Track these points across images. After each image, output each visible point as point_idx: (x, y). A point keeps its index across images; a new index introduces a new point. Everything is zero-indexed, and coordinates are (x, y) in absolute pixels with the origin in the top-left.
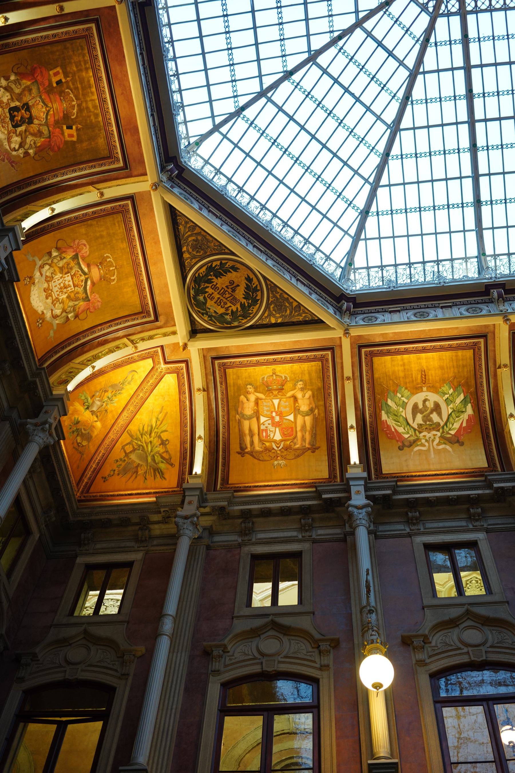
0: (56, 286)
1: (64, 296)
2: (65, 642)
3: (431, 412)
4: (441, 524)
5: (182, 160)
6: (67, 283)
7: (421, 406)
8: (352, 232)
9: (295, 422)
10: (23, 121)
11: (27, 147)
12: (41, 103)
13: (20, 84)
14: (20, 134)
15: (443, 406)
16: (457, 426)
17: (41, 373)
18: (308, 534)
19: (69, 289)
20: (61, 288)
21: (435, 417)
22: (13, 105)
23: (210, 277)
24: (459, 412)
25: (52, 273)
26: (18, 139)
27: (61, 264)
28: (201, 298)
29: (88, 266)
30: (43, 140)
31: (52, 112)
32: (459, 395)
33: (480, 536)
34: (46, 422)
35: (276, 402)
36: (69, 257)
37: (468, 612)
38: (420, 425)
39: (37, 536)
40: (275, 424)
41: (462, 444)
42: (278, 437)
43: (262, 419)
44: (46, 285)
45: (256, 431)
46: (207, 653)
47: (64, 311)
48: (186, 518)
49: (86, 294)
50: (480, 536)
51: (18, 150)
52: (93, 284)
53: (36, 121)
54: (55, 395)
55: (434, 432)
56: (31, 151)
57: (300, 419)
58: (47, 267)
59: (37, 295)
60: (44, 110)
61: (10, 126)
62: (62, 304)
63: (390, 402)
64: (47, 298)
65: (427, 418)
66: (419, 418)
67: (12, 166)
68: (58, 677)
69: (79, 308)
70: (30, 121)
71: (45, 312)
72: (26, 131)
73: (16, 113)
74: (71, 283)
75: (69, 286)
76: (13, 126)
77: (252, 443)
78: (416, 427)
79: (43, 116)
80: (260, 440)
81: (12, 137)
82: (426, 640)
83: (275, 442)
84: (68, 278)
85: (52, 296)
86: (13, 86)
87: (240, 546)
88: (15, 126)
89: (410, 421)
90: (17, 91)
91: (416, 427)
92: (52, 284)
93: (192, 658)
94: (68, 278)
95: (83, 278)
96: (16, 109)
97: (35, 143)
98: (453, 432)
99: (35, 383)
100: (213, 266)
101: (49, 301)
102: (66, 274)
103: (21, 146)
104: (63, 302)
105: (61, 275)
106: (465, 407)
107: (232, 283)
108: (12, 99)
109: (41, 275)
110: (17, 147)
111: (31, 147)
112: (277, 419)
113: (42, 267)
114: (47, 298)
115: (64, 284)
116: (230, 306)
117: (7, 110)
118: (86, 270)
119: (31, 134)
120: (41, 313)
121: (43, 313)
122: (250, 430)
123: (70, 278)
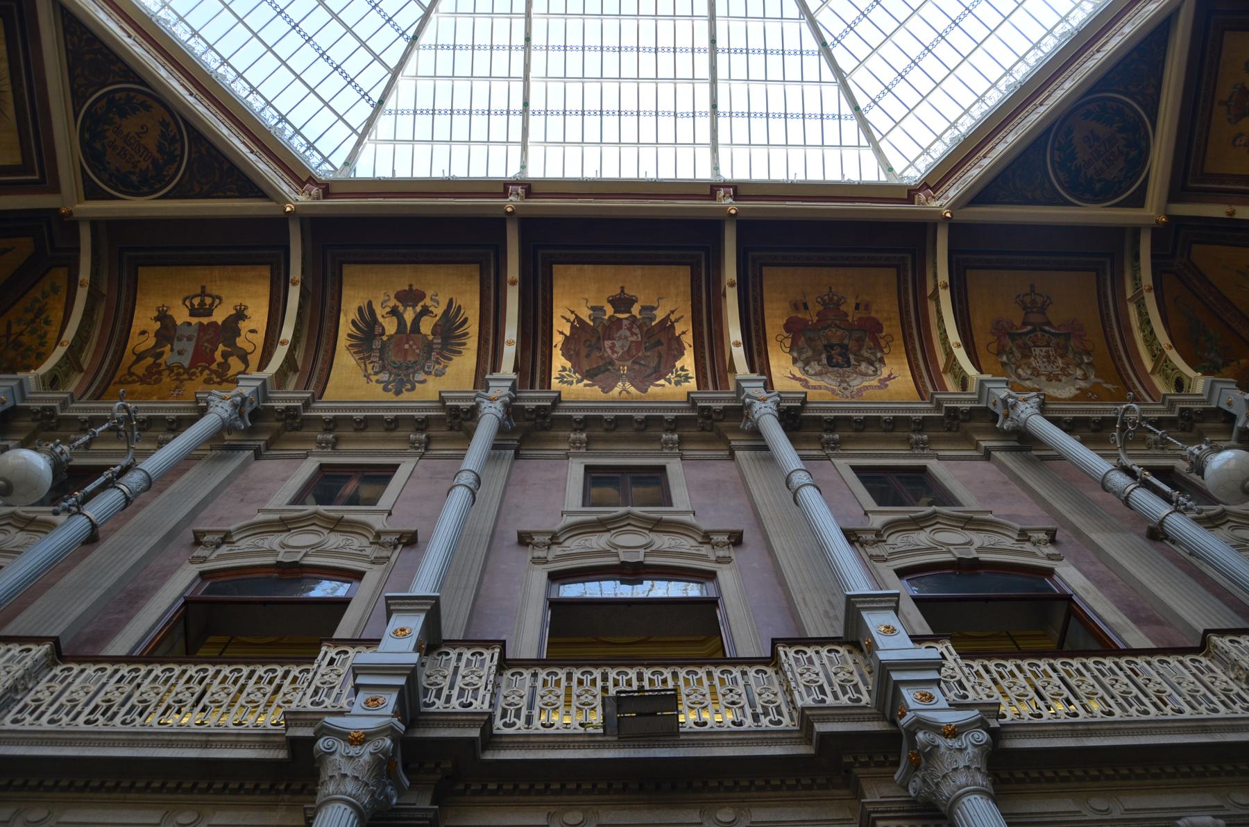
0: (1045, 367)
5: (913, 184)
6: (1043, 354)
11: (873, 359)
12: (827, 331)
13: (802, 349)
14: (859, 362)
17: (1170, 400)
19: (1051, 353)
20: (1049, 362)
22: (825, 361)
23: (1073, 168)
25: (1029, 367)
27: (1018, 355)
28: (1098, 186)
29: (1025, 324)
30: (867, 339)
31: (838, 322)
36: (1010, 344)
44: (1043, 378)
49: (1061, 334)
51: (876, 368)
52: (1049, 324)
53: (846, 341)
54: (1204, 390)
56: (879, 355)
58: (1020, 371)
59: (1055, 391)
60: (834, 330)
61: (848, 369)
62: (1071, 366)
64: (1060, 380)
67: (894, 378)
69: (1078, 348)
70: (844, 347)
71: (1077, 386)
72: (855, 355)
73: (834, 360)
74: (1044, 349)
75: (1047, 352)
76: (849, 366)
81: (860, 371)
85: (1058, 374)
86: (804, 356)
90: (810, 353)
92: (1042, 370)
94: (1037, 351)
95: (1039, 334)
96: (829, 359)
97: (870, 349)
99: (1182, 410)
100: (1059, 160)
102: (1031, 352)
103: (872, 364)
104: (1068, 365)
105: (1032, 358)
108: (819, 361)
109: (1028, 379)
110: (873, 369)
113: (1019, 376)
114: (1060, 380)
115: (1044, 357)
116: (1118, 147)
117: (830, 369)
118: (1029, 328)
119: (860, 349)
120: (1079, 392)
121: (1078, 389)
123: (1037, 350)
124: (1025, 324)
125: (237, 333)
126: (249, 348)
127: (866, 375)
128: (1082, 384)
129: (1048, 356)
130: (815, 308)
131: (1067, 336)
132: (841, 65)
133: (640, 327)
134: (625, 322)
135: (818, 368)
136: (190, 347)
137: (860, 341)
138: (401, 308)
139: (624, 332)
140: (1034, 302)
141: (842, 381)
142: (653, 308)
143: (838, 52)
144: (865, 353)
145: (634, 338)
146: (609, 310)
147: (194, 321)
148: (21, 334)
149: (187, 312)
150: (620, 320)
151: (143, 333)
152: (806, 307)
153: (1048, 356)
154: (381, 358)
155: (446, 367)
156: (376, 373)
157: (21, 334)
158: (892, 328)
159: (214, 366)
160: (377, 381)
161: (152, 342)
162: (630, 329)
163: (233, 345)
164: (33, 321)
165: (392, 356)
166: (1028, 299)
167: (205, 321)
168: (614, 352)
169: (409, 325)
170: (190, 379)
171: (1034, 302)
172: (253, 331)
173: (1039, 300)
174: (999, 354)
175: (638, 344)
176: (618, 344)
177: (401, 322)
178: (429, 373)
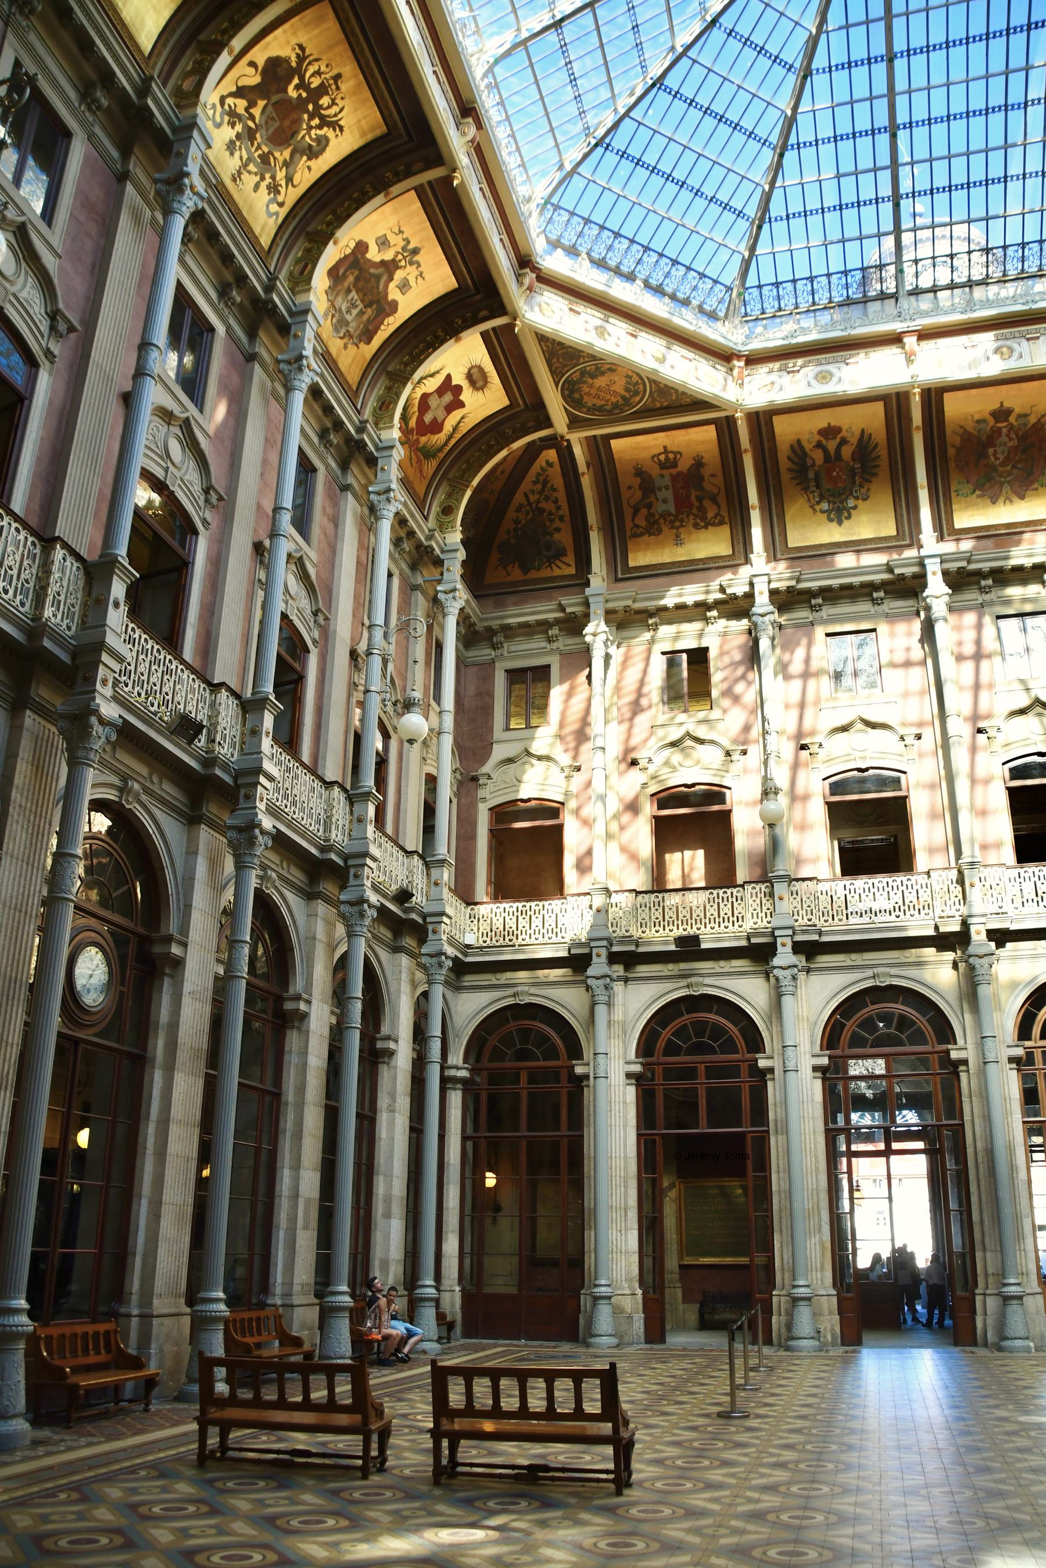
125: (701, 478)
126: (716, 491)
133: (1016, 433)
134: (1004, 430)
136: (669, 494)
138: (824, 442)
139: (1004, 438)
142: (1026, 416)
145: (1011, 444)
146: (991, 421)
147: (666, 472)
148: (538, 502)
149: (657, 467)
150: (1000, 429)
151: (630, 488)
154: (818, 487)
155: (868, 490)
156: (818, 503)
157: (538, 502)
159: (695, 511)
160: (822, 512)
161: (639, 494)
162: (1008, 435)
163: (702, 489)
164: (543, 490)
165: (826, 485)
167: (673, 471)
168: (997, 459)
169: (832, 453)
170: (682, 526)
172: (712, 476)
175: (1015, 449)
176: (999, 450)
177: (825, 451)
178: (857, 498)
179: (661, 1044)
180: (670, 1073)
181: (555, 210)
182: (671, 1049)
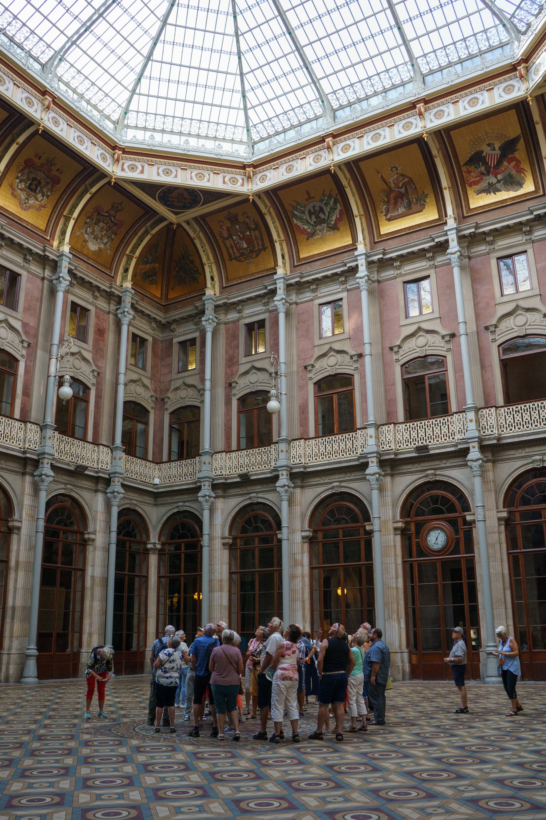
1: (105, 232)
2: (177, 389)
3: (319, 213)
4: (327, 289)
7: (312, 211)
8: (242, 106)
9: (251, 235)
10: (37, 186)
14: (40, 192)
15: (324, 207)
16: (334, 218)
18: (267, 307)
21: (322, 216)
22: (28, 185)
24: (333, 209)
26: (40, 195)
27: (94, 222)
29: (107, 212)
32: (331, 199)
33: (344, 295)
34: (124, 312)
35: (237, 227)
37: (331, 348)
38: (315, 222)
39: (150, 339)
40: (241, 239)
41: (338, 229)
42: (245, 246)
43: (234, 238)
44: (93, 236)
45: (233, 245)
46: (230, 385)
47: (108, 238)
48: (206, 321)
50: (344, 295)
52: (114, 217)
55: (323, 225)
57: (252, 232)
58: (89, 229)
63: (296, 212)
65: (318, 217)
66: (313, 217)
68: (179, 406)
70: (40, 182)
77: (234, 253)
78: (313, 223)
79: (43, 176)
80: (238, 250)
82: (313, 366)
83: (244, 249)
84: (101, 224)
86: (22, 178)
87: (238, 320)
88: (36, 190)
89: (309, 221)
90: (25, 178)
91: (313, 223)
93: (226, 388)
94: (101, 224)
96: (31, 184)
98: (333, 223)
101: (99, 240)
103: (43, 196)
104: (105, 234)
106: (336, 205)
107: (179, 194)
108: (26, 183)
111: (47, 192)
112: (241, 235)
113: (86, 231)
117: (27, 190)
122: (231, 246)
124: (107, 212)
127: (37, 200)
128: (102, 246)
129: (102, 228)
130: (43, 160)
131: (116, 224)
132: (155, 52)
135: (23, 186)
137: (47, 183)
140: (117, 207)
141: (27, 199)
143: (159, 45)
144: (45, 191)
152: (40, 158)
153: (102, 228)
158: (61, 186)
166: (116, 205)
171: (117, 207)
173: (120, 208)
174: (88, 218)
179: (518, 496)
180: (525, 515)
181: (515, 17)
182: (525, 502)
